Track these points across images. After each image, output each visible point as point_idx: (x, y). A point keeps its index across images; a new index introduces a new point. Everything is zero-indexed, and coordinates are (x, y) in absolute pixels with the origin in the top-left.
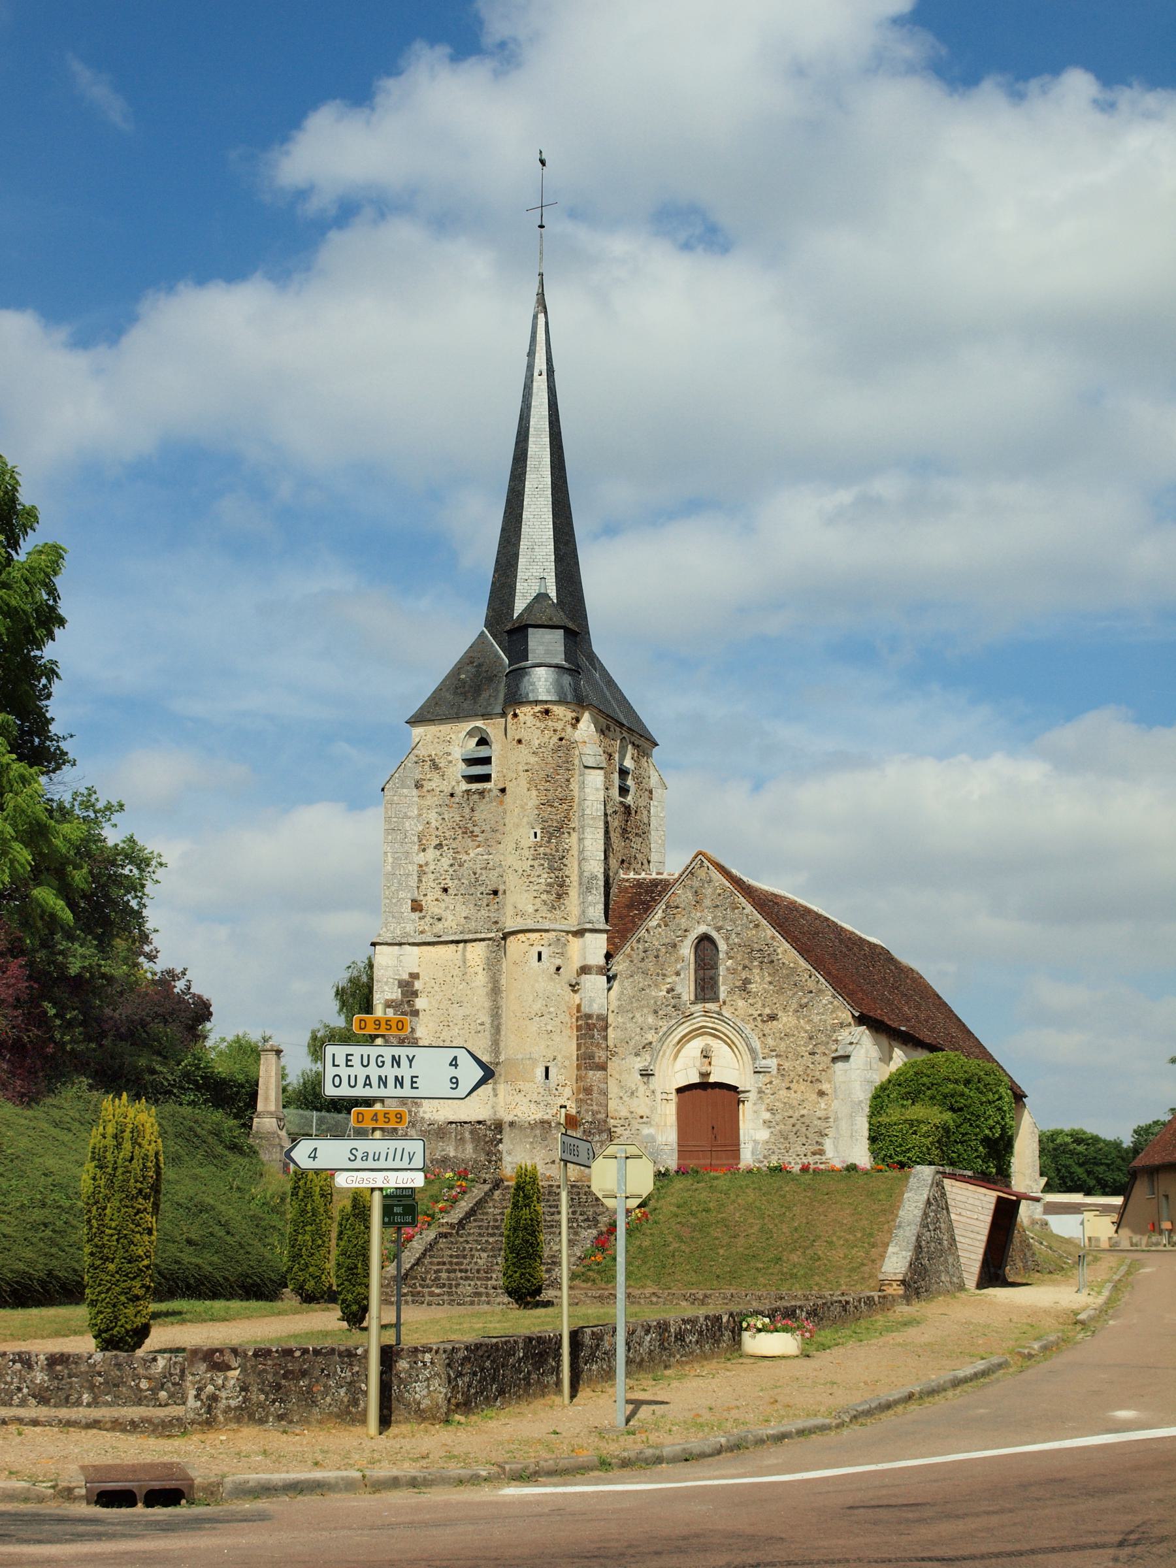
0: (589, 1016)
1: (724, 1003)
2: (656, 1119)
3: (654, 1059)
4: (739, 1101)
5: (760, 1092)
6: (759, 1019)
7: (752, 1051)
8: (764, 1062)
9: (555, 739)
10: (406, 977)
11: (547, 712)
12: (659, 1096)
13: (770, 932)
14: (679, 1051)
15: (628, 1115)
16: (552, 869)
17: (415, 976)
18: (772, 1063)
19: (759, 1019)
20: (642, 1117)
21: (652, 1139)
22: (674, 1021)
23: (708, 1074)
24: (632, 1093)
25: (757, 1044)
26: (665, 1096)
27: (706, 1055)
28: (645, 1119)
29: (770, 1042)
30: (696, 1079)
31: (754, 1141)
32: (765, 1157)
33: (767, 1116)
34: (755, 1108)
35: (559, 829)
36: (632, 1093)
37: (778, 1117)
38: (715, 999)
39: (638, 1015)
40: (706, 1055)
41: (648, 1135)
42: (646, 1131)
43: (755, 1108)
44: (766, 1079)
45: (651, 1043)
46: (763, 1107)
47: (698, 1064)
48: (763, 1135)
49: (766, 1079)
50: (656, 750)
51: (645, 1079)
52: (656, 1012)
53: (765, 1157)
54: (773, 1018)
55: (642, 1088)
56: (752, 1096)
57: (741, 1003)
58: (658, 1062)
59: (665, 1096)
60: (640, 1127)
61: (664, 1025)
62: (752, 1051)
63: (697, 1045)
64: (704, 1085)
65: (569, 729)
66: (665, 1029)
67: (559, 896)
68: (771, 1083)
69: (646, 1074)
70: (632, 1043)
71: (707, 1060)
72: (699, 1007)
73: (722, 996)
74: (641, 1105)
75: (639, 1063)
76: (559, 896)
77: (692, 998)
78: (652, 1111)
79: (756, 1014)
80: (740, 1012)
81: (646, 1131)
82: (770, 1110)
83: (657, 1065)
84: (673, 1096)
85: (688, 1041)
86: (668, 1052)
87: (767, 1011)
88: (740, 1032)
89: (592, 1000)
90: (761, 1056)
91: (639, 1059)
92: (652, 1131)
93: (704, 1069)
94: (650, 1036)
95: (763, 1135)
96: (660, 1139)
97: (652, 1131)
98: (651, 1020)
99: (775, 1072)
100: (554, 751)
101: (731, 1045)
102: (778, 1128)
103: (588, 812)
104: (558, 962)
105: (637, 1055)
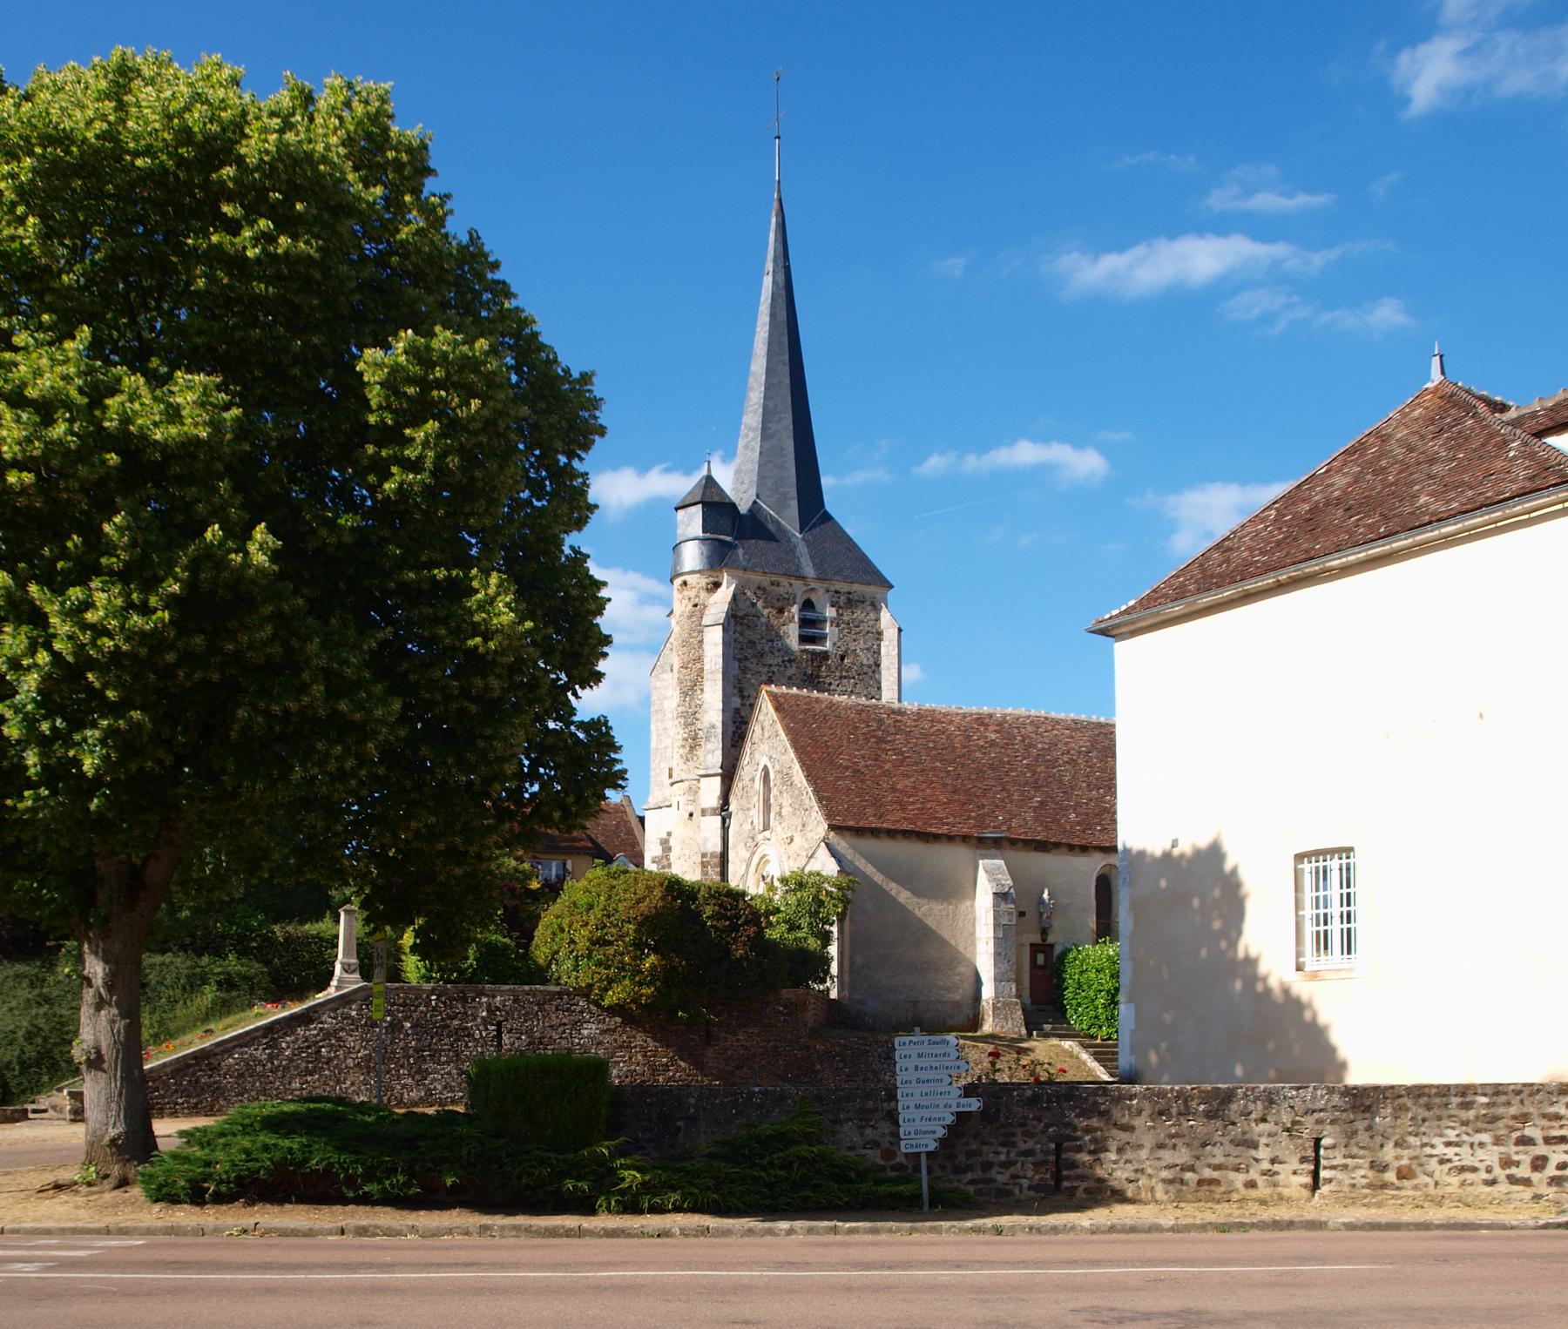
0: (704, 855)
9: (690, 606)
10: (665, 836)
11: (685, 583)
13: (791, 754)
16: (686, 725)
17: (669, 834)
35: (692, 688)
50: (891, 593)
65: (703, 594)
67: (692, 748)
76: (692, 748)
89: (706, 840)
100: (690, 617)
103: (706, 667)
104: (691, 809)
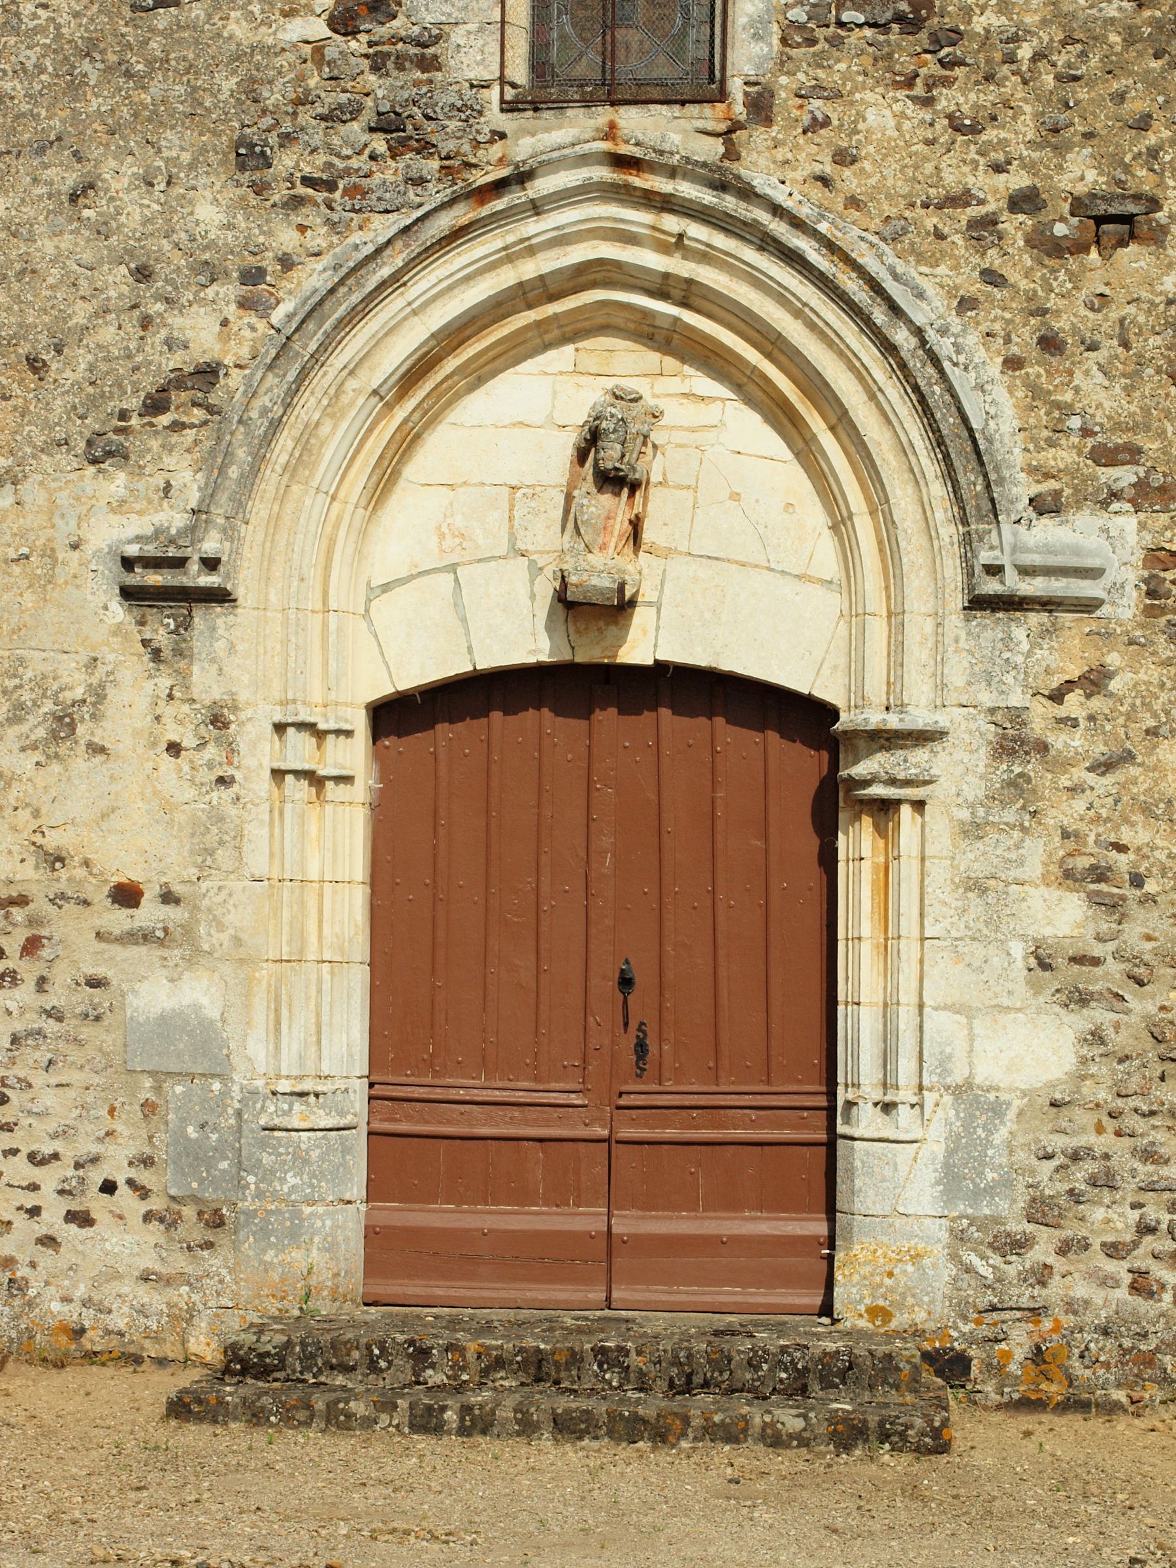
1: (761, 107)
2: (234, 907)
3: (229, 489)
4: (831, 804)
5: (1013, 742)
6: (1015, 226)
7: (960, 450)
8: (1046, 535)
12: (258, 751)
14: (407, 442)
15: (31, 876)
18: (1110, 542)
19: (1015, 226)
20: (127, 895)
21: (198, 1051)
22: (383, 227)
23: (618, 608)
24: (64, 724)
25: (997, 407)
26: (300, 751)
27: (608, 464)
28: (149, 913)
29: (1097, 392)
30: (521, 637)
31: (962, 1091)
32: (1041, 1211)
33: (1066, 917)
34: (975, 859)
36: (64, 724)
37: (1142, 929)
38: (708, 87)
39: (118, 176)
40: (608, 464)
41: (168, 1025)
42: (155, 992)
43: (975, 859)
44: (1065, 655)
45: (208, 373)
46: (1037, 854)
47: (544, 534)
48: (1032, 1050)
49: (1065, 655)
51: (160, 632)
52: (250, 157)
53: (1041, 1211)
54: (1116, 222)
55: (135, 692)
56: (958, 772)
57: (882, 115)
58: (260, 508)
59: (300, 751)
60: (115, 963)
61: (313, 254)
62: (960, 450)
63: (536, 406)
64: (585, 682)
66: (313, 277)
68: (1094, 681)
69: (170, 590)
70: (73, 370)
71: (610, 509)
72: (574, 128)
73: (748, 57)
74: (123, 811)
75: (117, 515)
77: (519, 72)
78: (204, 871)
79: (994, 190)
80: (880, 175)
81: (155, 992)
82: (1089, 877)
83: (253, 534)
84: (354, 755)
85: (479, 374)
86: (335, 441)
87: (1081, 173)
88: (873, 311)
90: (1021, 489)
91: (118, 482)
92: (198, 993)
93: (597, 572)
94: (205, 328)
95: (1032, 1050)
96: (256, 1057)
97: (198, 993)
98: (211, 210)
99: (1126, 608)
101: (792, 407)
102: (1142, 1005)
105: (103, 453)
